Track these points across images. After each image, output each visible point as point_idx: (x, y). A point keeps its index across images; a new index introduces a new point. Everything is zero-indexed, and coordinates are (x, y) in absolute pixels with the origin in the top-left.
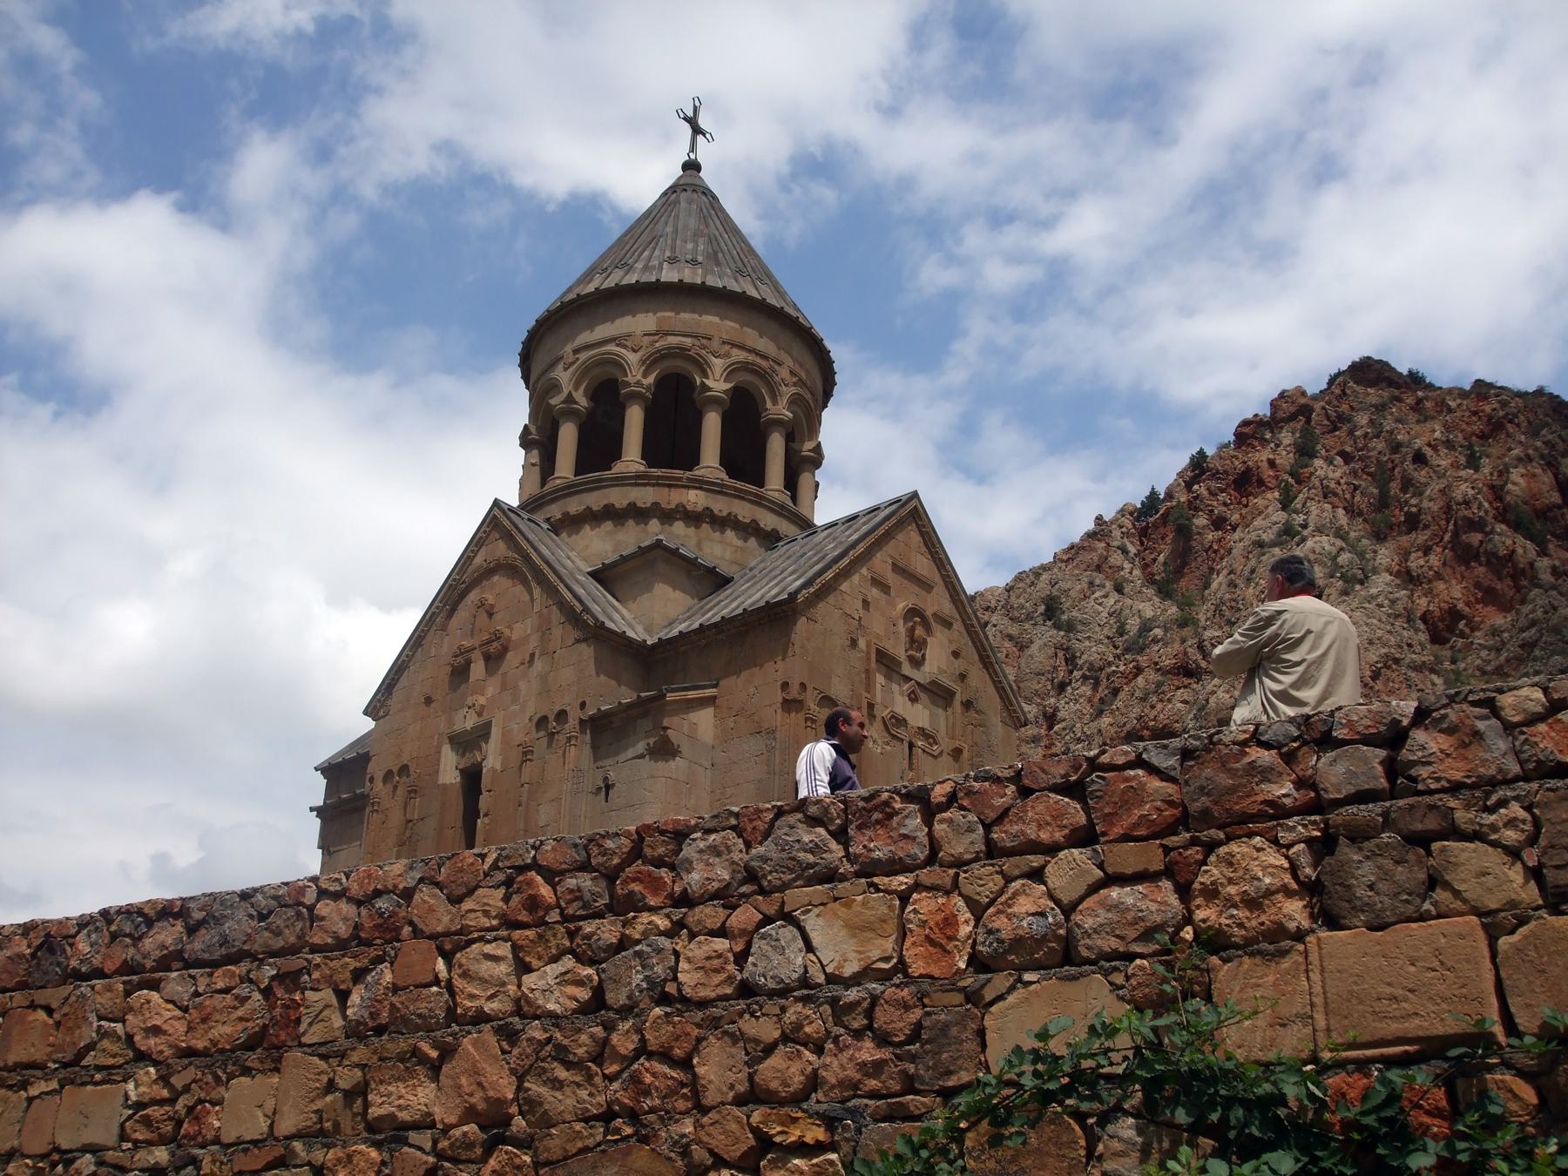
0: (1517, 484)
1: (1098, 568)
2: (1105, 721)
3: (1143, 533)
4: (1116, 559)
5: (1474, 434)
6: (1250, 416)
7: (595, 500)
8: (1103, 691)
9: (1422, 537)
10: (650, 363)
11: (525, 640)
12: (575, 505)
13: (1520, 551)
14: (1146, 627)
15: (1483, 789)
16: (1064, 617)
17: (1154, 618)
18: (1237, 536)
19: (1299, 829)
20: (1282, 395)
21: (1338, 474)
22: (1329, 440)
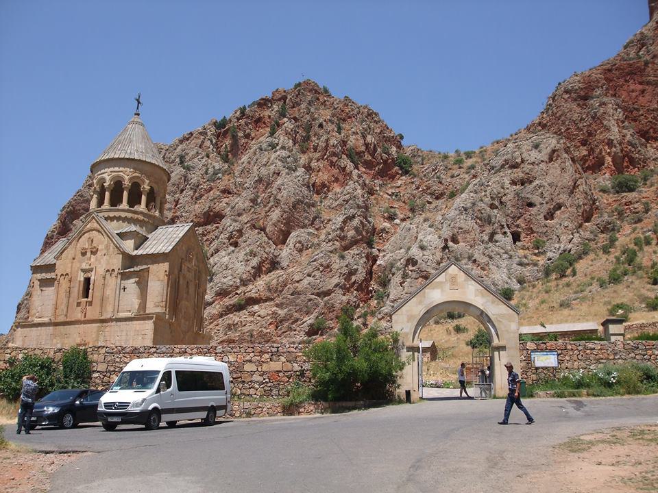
0: (352, 141)
1: (200, 147)
2: (197, 206)
3: (218, 136)
4: (208, 143)
5: (341, 119)
6: (264, 97)
7: (117, 214)
8: (197, 195)
9: (318, 155)
10: (130, 179)
11: (102, 250)
12: (111, 214)
13: (349, 167)
14: (215, 174)
15: (283, 353)
16: (186, 164)
17: (220, 169)
18: (253, 142)
19: (270, 354)
20: (277, 90)
21: (292, 126)
22: (290, 111)
